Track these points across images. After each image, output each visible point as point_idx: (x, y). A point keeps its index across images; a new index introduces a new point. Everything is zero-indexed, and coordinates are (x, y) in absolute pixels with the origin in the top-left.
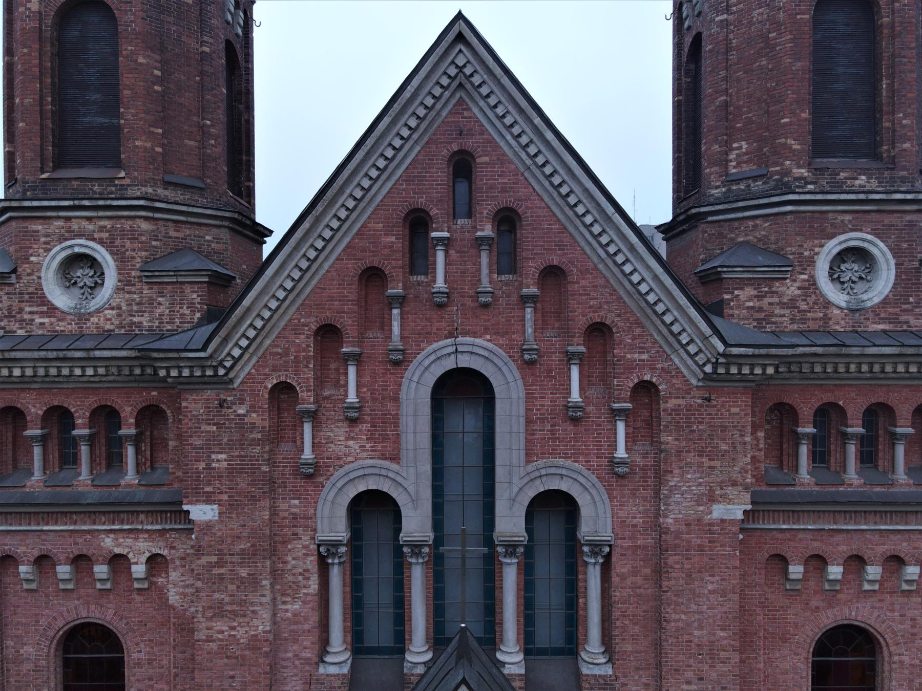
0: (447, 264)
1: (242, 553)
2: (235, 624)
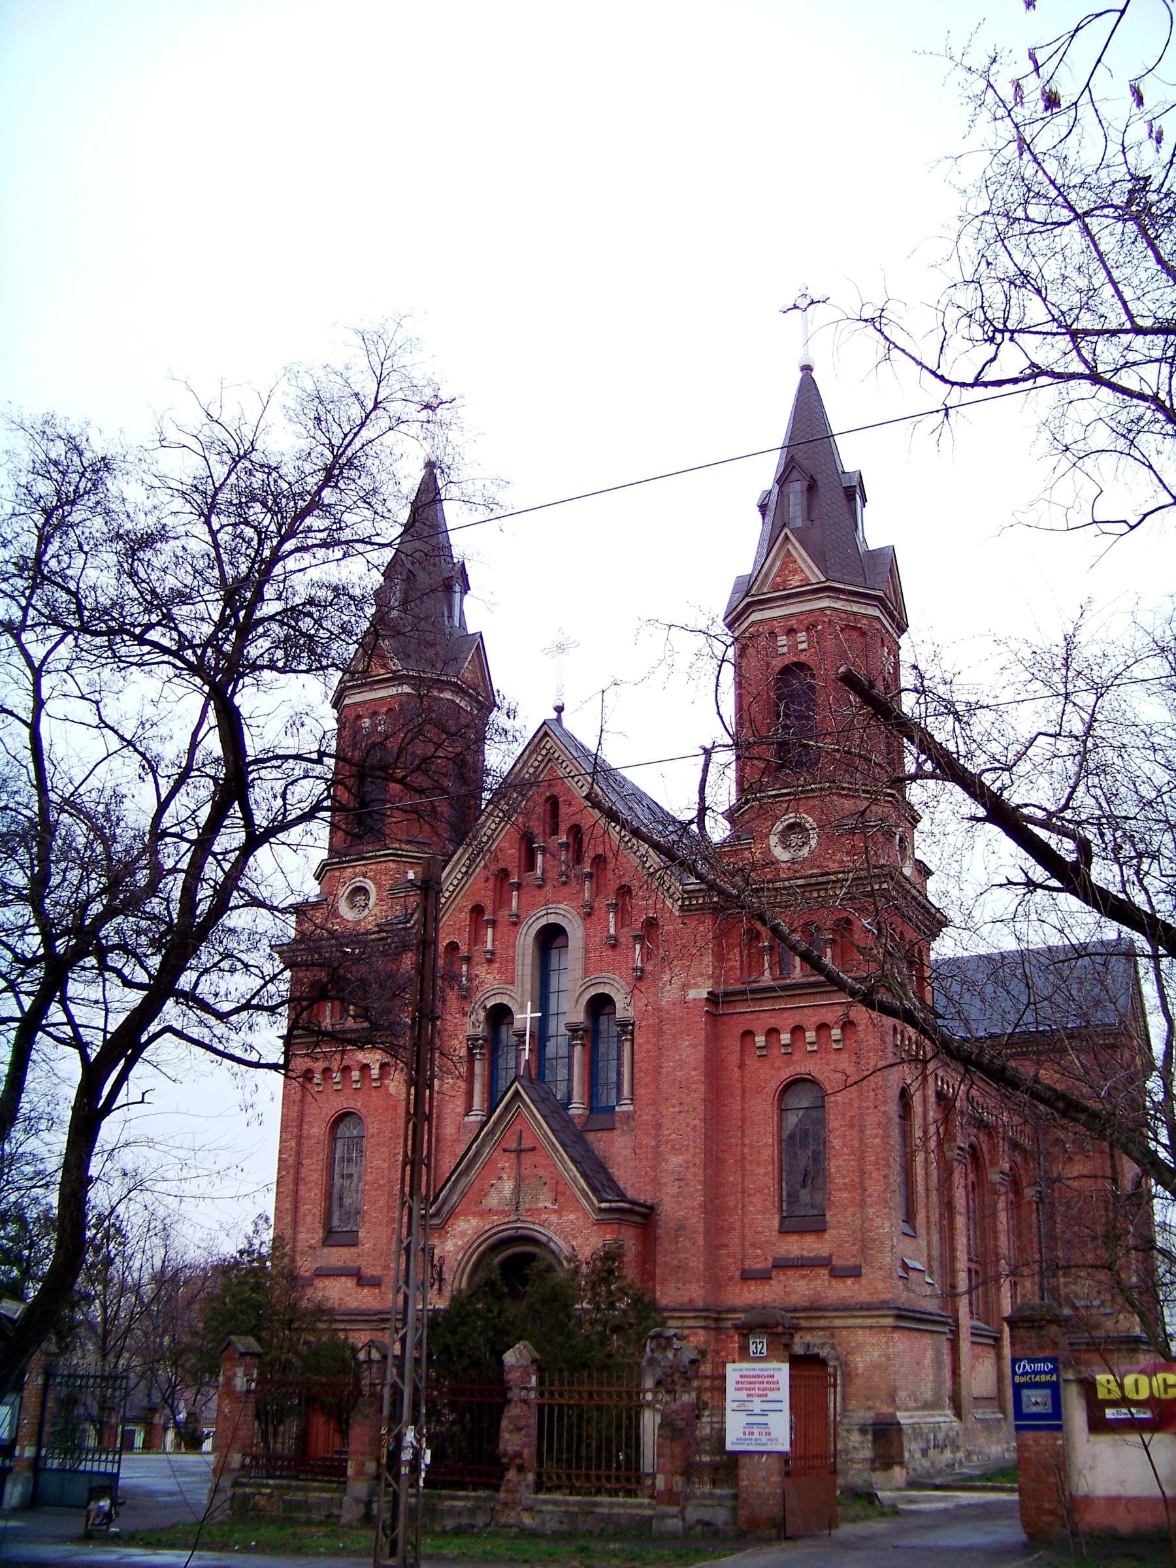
0: (544, 862)
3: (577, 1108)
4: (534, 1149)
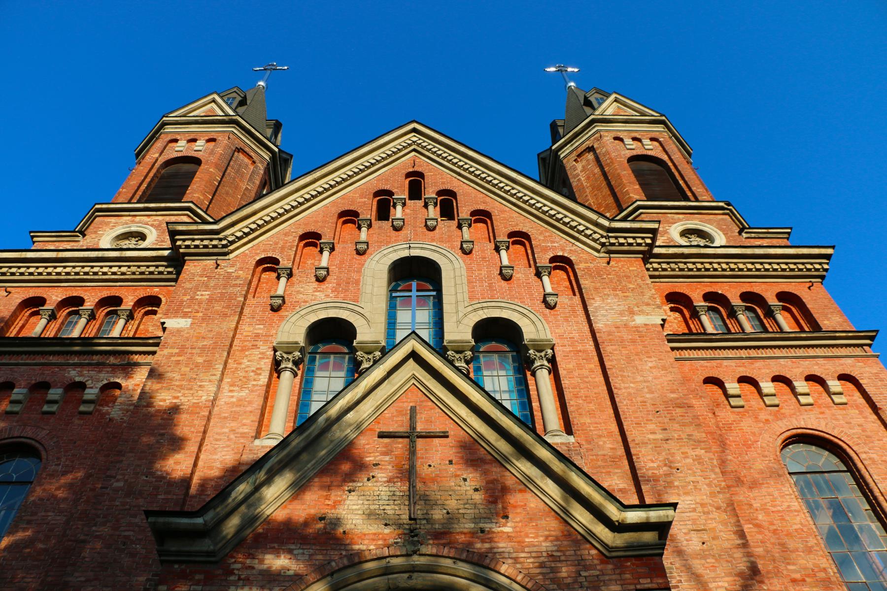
1: (203, 348)
2: (179, 395)
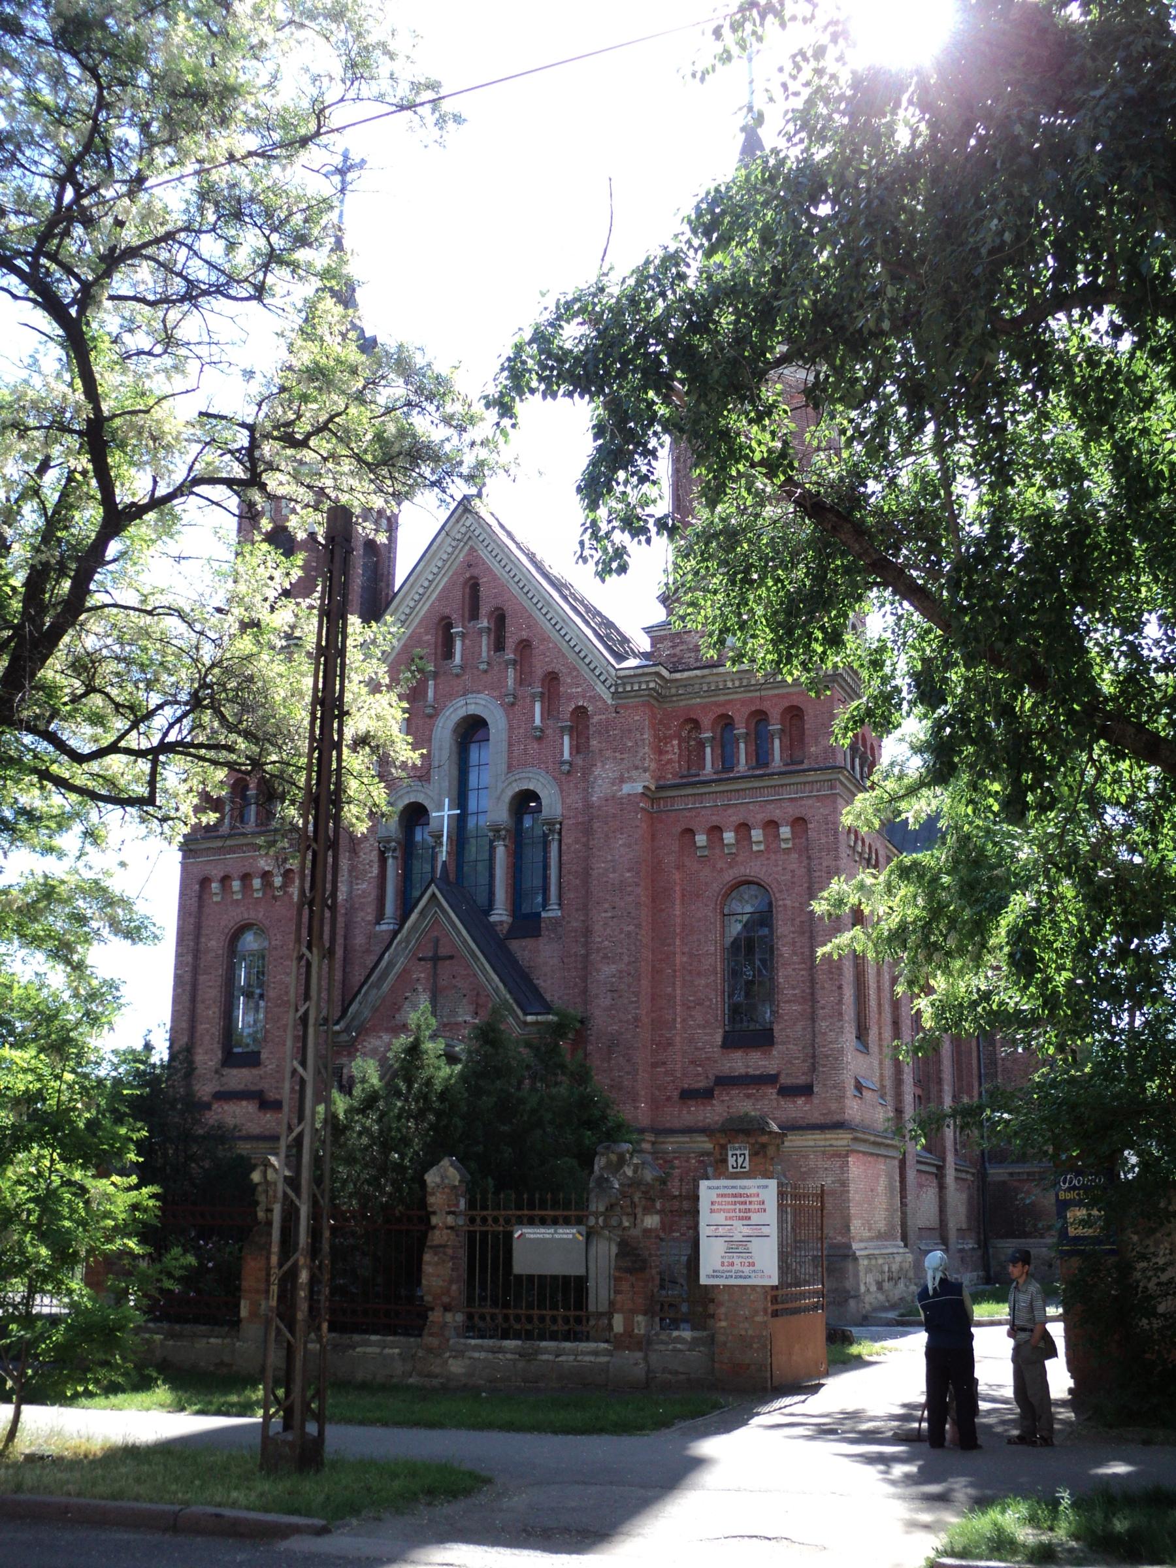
0: (463, 650)
3: (500, 914)
4: (451, 957)
